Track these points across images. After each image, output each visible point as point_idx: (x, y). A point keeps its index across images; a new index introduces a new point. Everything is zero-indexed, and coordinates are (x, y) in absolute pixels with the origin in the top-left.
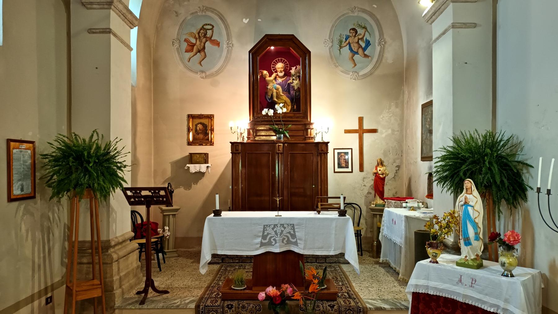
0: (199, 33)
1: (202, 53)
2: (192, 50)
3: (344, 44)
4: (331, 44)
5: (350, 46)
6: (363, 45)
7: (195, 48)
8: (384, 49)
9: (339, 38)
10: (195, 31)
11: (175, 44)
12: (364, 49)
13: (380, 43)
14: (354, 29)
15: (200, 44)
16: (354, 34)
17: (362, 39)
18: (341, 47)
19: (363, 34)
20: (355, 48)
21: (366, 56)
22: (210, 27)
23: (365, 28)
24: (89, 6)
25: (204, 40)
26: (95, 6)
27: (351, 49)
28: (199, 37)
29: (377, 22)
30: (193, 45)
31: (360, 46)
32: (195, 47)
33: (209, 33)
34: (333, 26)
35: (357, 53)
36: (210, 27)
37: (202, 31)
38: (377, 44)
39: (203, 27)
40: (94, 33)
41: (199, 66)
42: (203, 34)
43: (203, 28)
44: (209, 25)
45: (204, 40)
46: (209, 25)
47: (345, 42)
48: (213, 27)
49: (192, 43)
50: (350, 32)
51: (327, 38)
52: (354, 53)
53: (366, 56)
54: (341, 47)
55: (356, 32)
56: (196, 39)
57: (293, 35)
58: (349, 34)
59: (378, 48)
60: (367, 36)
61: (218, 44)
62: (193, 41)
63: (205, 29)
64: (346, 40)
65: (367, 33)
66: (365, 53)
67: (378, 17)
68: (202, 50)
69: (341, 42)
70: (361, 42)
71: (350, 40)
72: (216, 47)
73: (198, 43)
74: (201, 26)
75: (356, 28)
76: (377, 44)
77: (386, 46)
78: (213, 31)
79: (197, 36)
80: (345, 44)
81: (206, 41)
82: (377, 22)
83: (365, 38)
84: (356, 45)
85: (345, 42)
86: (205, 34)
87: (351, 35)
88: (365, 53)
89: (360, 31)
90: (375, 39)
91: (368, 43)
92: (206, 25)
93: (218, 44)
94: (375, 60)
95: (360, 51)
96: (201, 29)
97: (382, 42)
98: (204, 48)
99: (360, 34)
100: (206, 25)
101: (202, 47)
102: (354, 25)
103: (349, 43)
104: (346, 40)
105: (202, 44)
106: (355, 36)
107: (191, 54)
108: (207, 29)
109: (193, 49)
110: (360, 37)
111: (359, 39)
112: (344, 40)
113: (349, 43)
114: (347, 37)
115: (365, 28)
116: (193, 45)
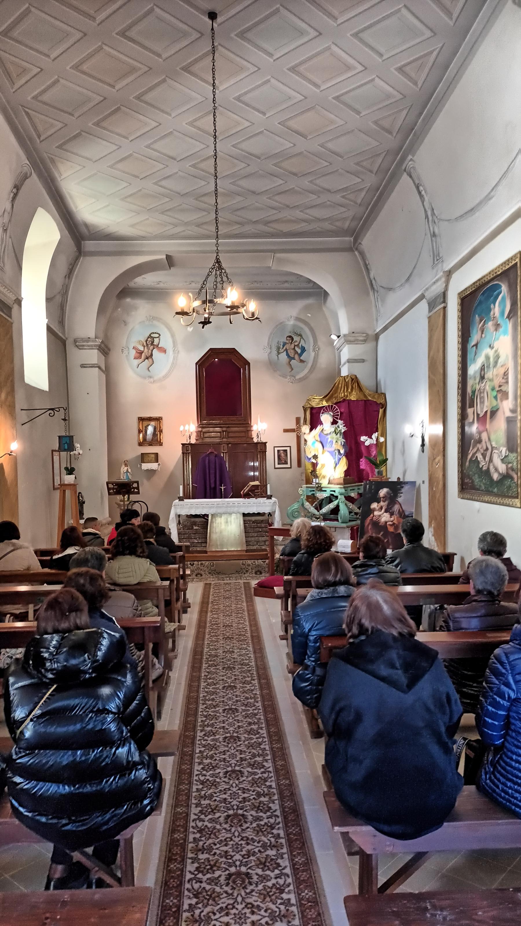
0: (146, 341)
1: (150, 360)
2: (140, 357)
3: (281, 350)
4: (269, 351)
5: (287, 352)
6: (299, 351)
7: (143, 356)
8: (318, 355)
9: (276, 344)
10: (143, 340)
11: (125, 352)
12: (300, 355)
13: (314, 350)
14: (290, 337)
15: (148, 352)
16: (290, 341)
17: (298, 345)
18: (279, 353)
19: (298, 342)
20: (292, 355)
21: (302, 361)
22: (157, 335)
23: (300, 335)
24: (81, 347)
25: (151, 347)
26: (86, 347)
27: (288, 355)
28: (147, 344)
29: (312, 330)
30: (141, 353)
31: (296, 352)
32: (143, 354)
33: (156, 341)
34: (271, 334)
35: (294, 358)
36: (157, 335)
37: (149, 339)
38: (311, 350)
39: (150, 335)
40: (85, 367)
41: (147, 371)
42: (150, 342)
43: (150, 336)
44: (155, 333)
45: (151, 347)
46: (155, 333)
47: (283, 348)
48: (160, 335)
49: (140, 351)
50: (287, 340)
51: (266, 345)
52: (291, 358)
53: (302, 361)
54: (279, 353)
55: (293, 339)
56: (144, 347)
57: (234, 349)
58: (285, 341)
59: (313, 354)
60: (302, 343)
61: (165, 351)
62: (142, 348)
63: (152, 337)
64: (283, 346)
65: (302, 341)
66: (301, 358)
67: (312, 325)
68: (150, 357)
69: (278, 348)
70: (297, 349)
71: (287, 346)
72: (163, 354)
73: (146, 350)
74: (148, 335)
75: (293, 336)
76: (311, 350)
77: (320, 352)
78: (160, 339)
79: (145, 344)
80: (282, 351)
81: (154, 348)
82: (312, 330)
83: (300, 345)
84: (292, 351)
85: (283, 348)
86: (153, 342)
87: (288, 342)
88: (301, 358)
89: (296, 338)
90: (309, 345)
91: (303, 350)
92: (153, 333)
93: (165, 351)
94: (310, 365)
95: (296, 357)
96: (148, 338)
97: (316, 348)
98: (152, 355)
99: (296, 341)
100: (153, 333)
101: (149, 354)
102: (290, 332)
103: (286, 350)
104: (283, 346)
105: (150, 351)
106: (291, 343)
107: (140, 361)
108: (154, 338)
109: (141, 356)
110: (296, 344)
111: (295, 346)
112: (282, 347)
113: (286, 350)
114: (284, 344)
115: (300, 335)
116: (141, 353)
